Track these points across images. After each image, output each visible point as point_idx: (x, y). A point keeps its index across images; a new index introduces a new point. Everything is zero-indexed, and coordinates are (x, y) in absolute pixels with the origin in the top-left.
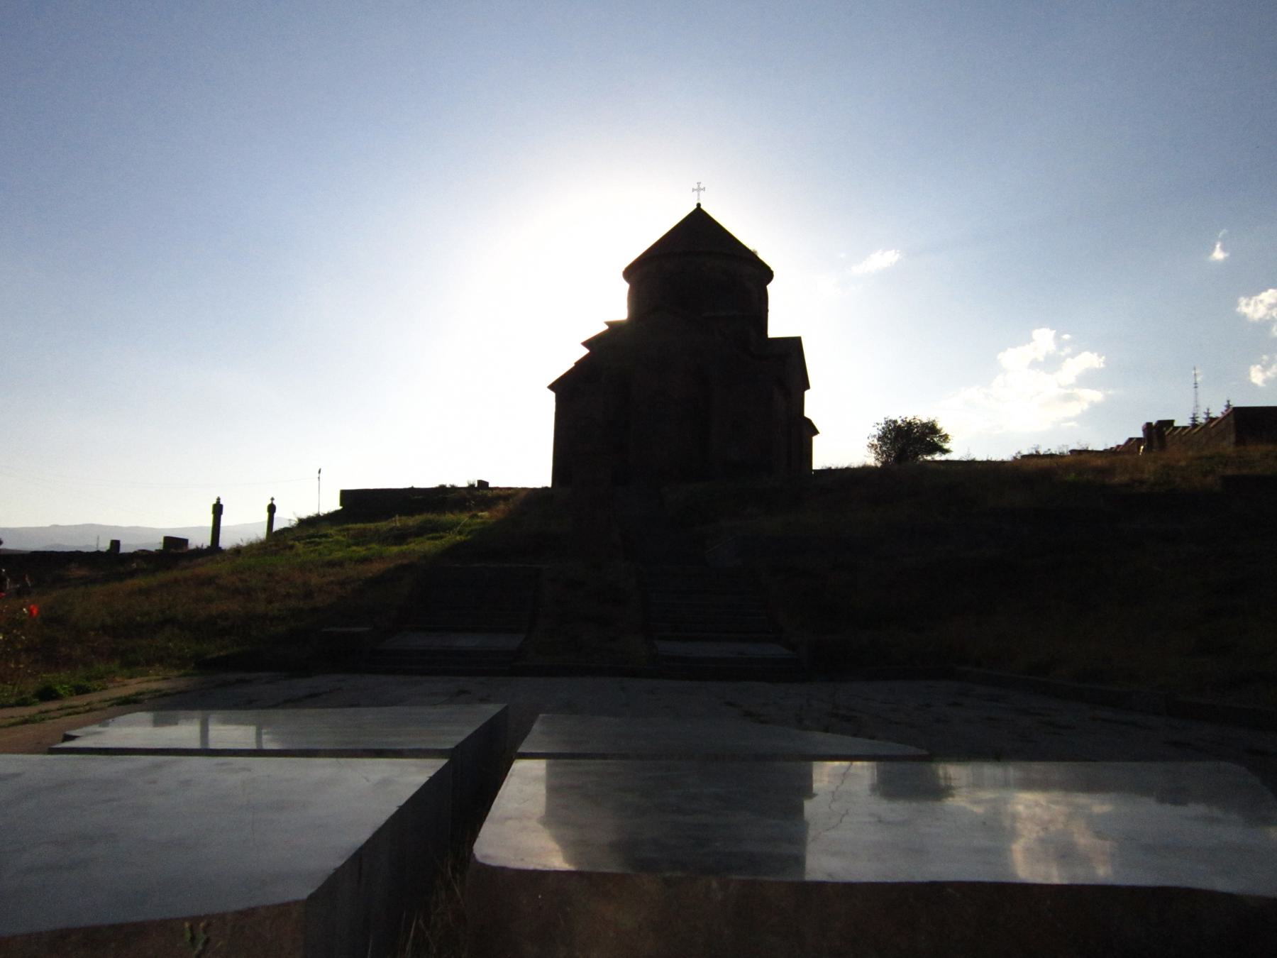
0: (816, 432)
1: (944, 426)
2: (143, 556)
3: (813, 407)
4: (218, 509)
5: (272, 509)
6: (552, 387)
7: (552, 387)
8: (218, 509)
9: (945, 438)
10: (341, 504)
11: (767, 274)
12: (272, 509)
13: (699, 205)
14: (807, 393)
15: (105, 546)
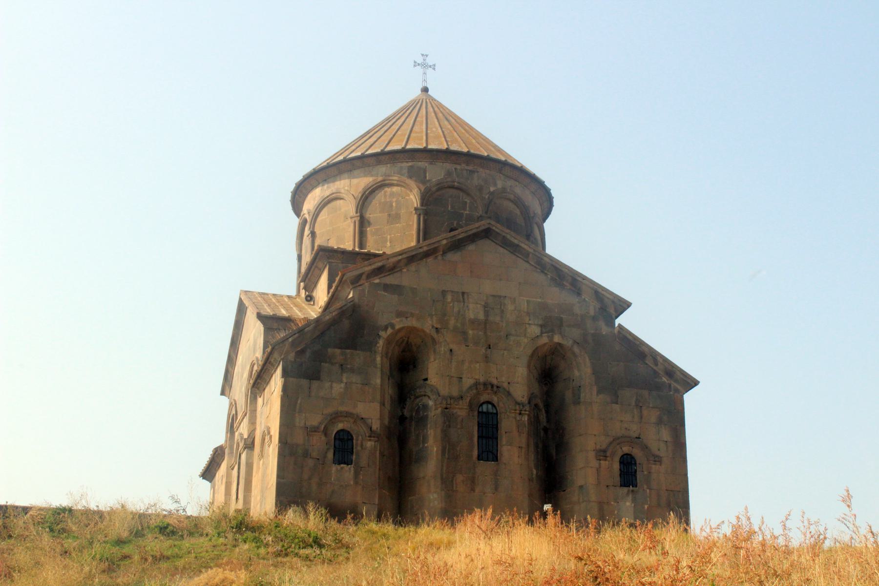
13: (425, 90)
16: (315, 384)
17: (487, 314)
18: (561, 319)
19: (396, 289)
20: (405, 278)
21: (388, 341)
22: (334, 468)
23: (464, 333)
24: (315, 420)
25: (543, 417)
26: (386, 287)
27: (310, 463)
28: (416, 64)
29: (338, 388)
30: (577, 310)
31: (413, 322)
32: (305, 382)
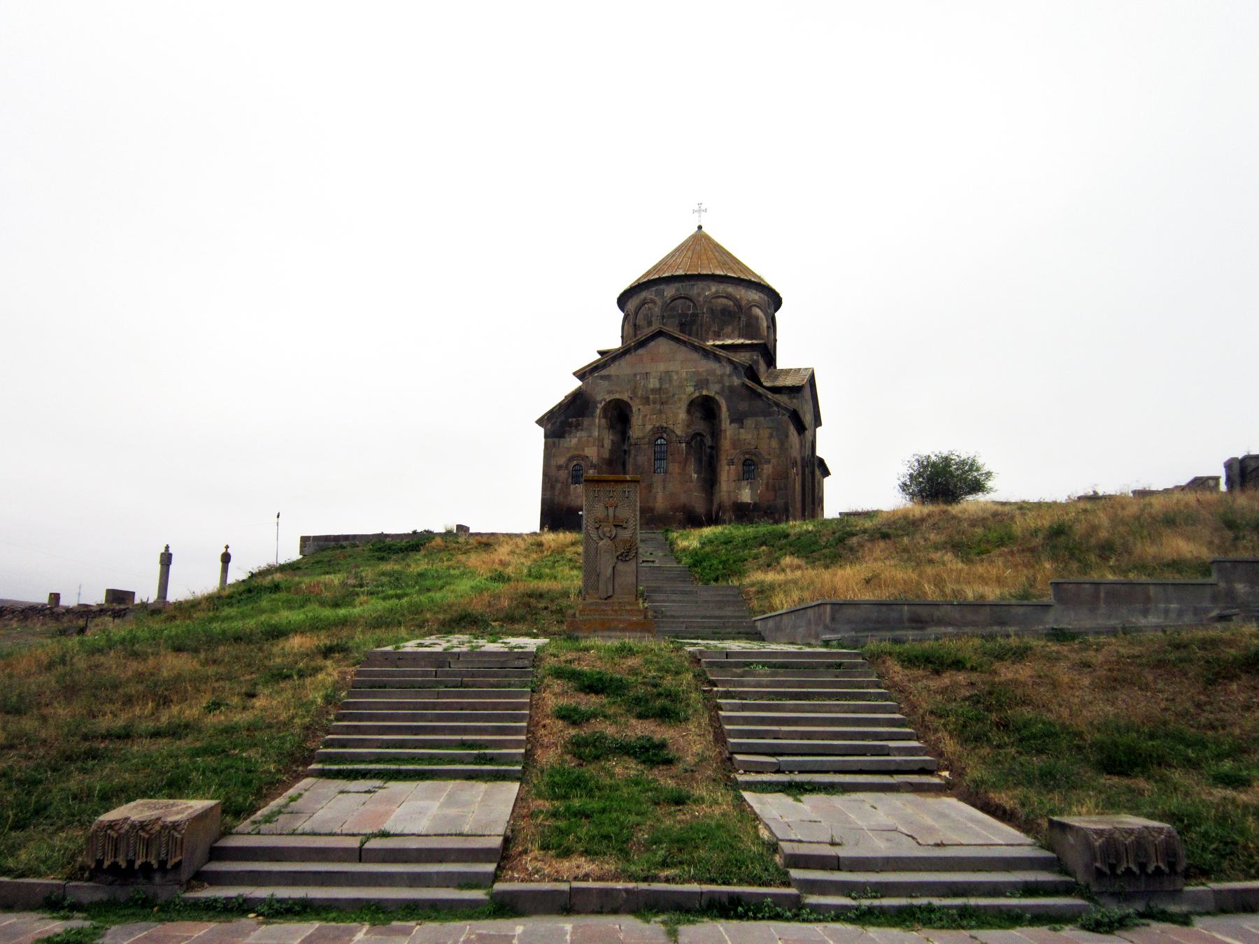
0: (826, 472)
1: (986, 462)
2: (85, 612)
3: (826, 444)
4: (166, 559)
5: (226, 558)
6: (540, 422)
7: (540, 422)
8: (166, 559)
9: (988, 474)
10: (301, 552)
11: (775, 300)
12: (226, 558)
13: (700, 227)
14: (818, 430)
15: (44, 599)
16: (562, 440)
17: (661, 383)
18: (707, 381)
19: (607, 378)
20: (612, 370)
21: (605, 409)
22: (572, 486)
23: (648, 398)
24: (562, 461)
25: (708, 441)
26: (602, 377)
27: (559, 485)
28: (694, 211)
29: (574, 441)
30: (718, 372)
31: (617, 396)
32: (556, 440)
